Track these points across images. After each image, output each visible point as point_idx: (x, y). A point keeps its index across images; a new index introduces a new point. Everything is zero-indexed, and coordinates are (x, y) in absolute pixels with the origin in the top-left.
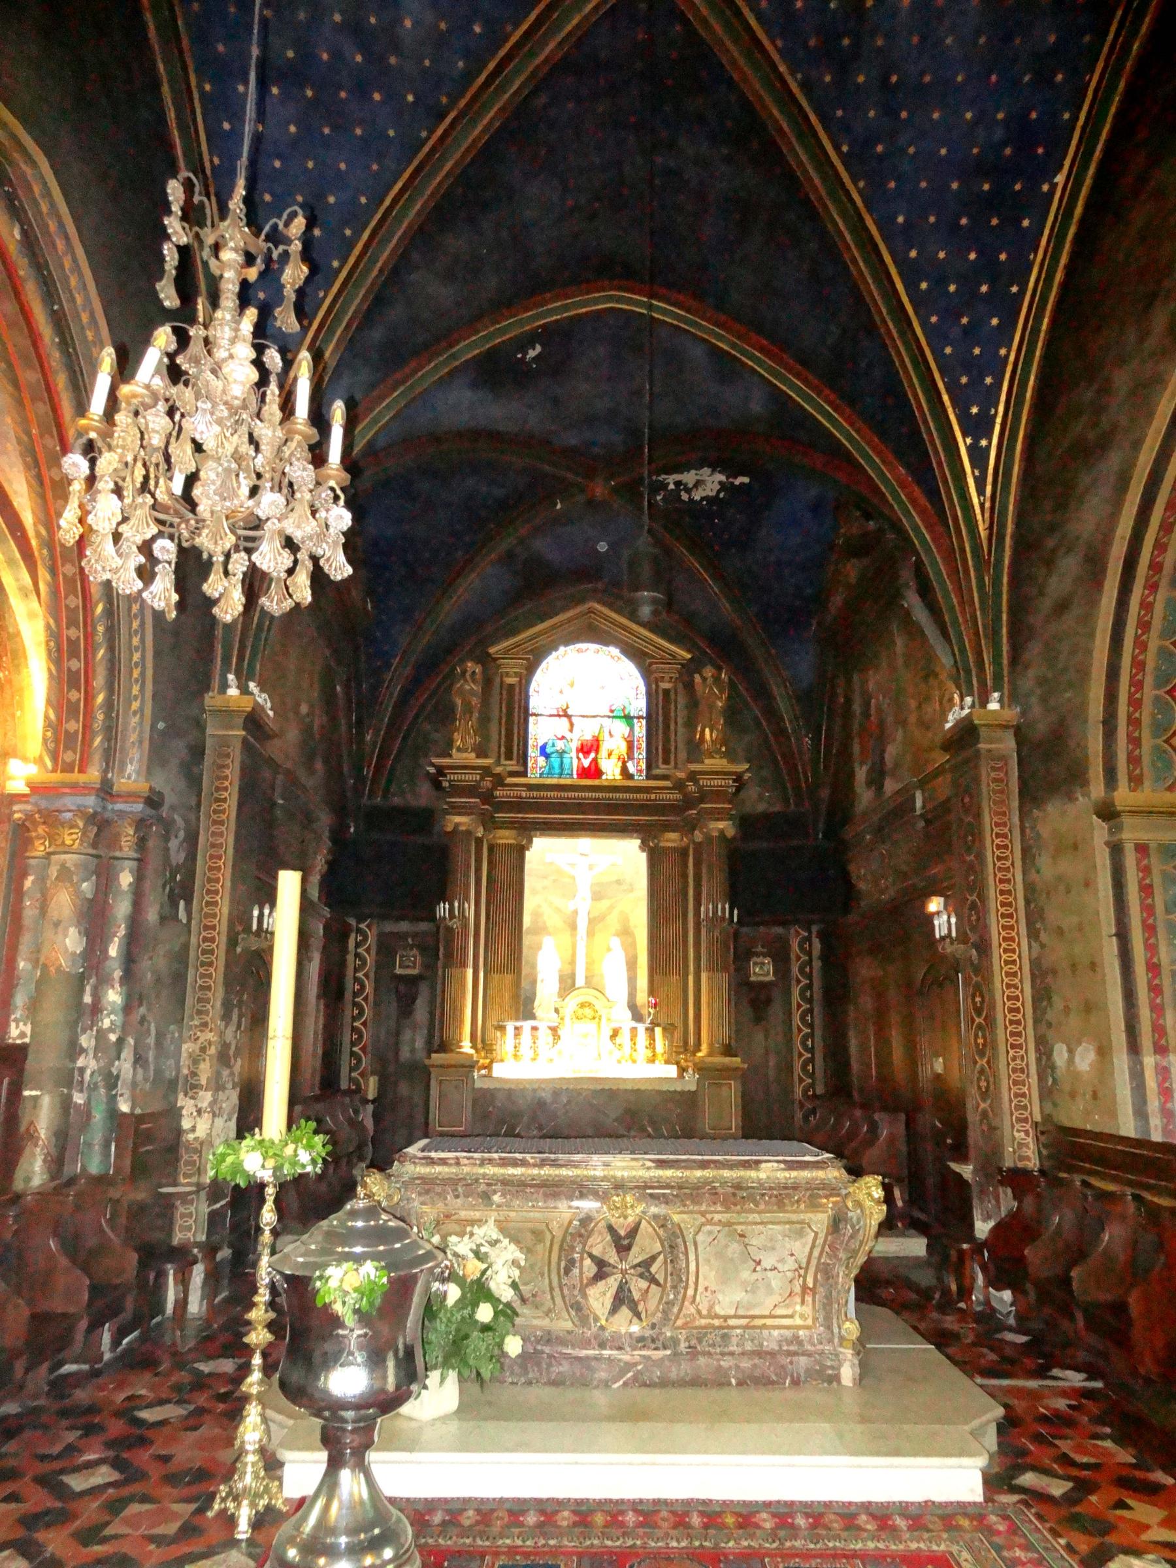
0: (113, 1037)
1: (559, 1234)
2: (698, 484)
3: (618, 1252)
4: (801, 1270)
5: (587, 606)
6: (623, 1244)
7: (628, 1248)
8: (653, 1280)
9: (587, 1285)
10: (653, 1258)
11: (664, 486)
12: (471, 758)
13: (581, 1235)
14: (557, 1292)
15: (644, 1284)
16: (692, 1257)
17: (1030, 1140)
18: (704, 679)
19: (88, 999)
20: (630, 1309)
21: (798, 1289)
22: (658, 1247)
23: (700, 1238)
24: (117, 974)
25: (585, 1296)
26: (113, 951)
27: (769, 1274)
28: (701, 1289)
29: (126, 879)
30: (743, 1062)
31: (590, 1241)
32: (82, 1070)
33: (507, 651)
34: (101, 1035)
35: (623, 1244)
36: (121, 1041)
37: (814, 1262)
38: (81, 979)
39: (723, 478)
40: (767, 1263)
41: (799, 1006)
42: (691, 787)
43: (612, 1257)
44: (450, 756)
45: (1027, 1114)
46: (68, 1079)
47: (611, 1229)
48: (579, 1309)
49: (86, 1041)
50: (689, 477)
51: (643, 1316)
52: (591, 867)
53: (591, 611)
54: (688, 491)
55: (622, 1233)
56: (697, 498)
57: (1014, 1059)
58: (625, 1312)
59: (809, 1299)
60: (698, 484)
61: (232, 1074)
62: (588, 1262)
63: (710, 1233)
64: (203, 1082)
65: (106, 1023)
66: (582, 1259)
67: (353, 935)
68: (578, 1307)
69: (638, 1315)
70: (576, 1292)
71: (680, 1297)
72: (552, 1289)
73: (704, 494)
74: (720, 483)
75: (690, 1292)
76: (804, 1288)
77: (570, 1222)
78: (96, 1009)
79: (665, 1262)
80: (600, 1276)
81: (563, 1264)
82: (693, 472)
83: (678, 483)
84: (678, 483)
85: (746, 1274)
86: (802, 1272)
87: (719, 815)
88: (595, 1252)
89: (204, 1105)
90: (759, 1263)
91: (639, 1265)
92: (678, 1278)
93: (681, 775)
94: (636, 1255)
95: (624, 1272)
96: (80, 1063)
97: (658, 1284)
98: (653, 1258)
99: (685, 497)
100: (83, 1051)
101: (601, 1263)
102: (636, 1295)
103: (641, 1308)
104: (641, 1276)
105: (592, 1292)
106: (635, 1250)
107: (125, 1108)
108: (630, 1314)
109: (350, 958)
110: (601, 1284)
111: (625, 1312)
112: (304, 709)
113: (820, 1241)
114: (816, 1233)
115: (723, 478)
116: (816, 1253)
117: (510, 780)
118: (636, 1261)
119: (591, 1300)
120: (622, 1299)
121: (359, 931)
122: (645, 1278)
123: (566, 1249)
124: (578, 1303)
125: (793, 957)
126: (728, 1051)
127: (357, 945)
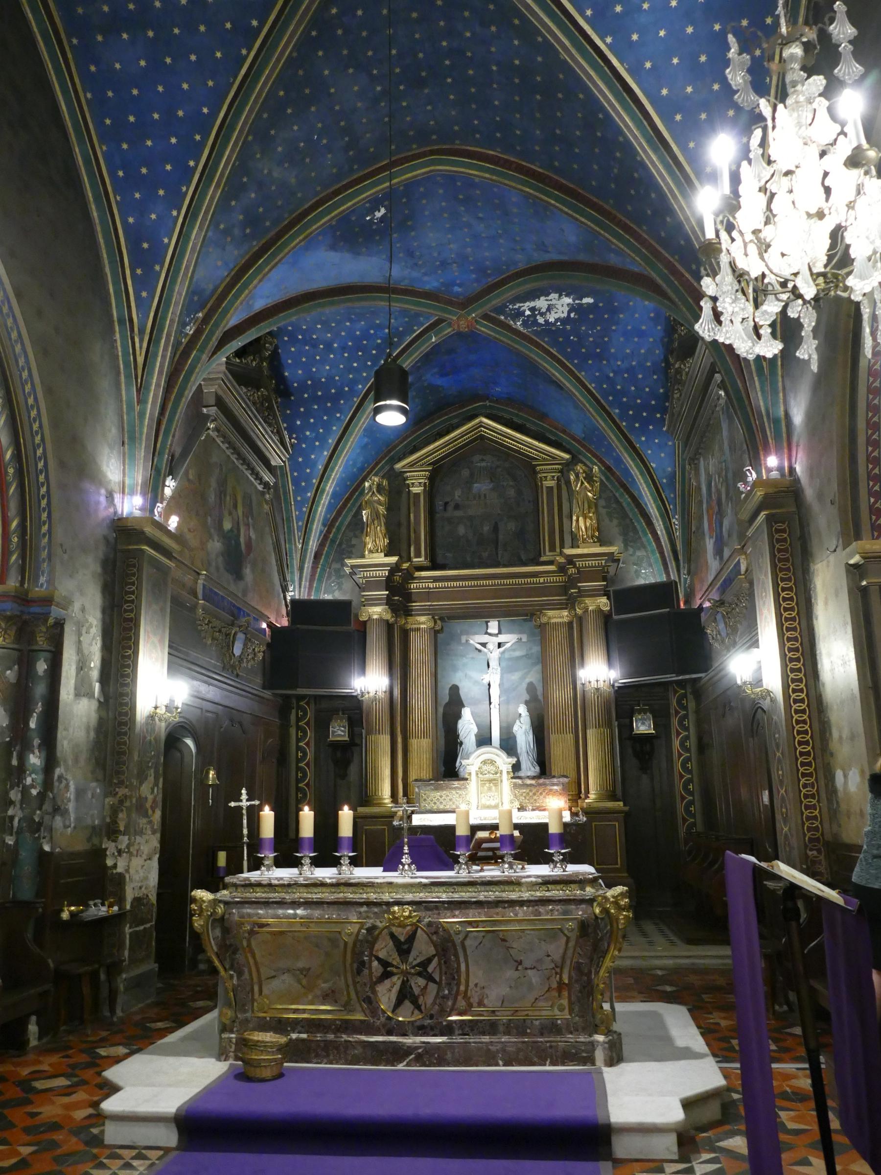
0: (34, 792)
1: (350, 941)
2: (549, 309)
3: (399, 955)
4: (559, 967)
5: (477, 421)
6: (404, 948)
7: (408, 952)
8: (430, 978)
9: (376, 983)
10: (429, 960)
11: (519, 314)
12: (380, 558)
13: (367, 942)
14: (351, 988)
15: (421, 982)
16: (462, 959)
17: (822, 857)
18: (577, 476)
19: (15, 762)
20: (412, 1002)
21: (555, 985)
22: (432, 951)
23: (468, 943)
24: (36, 742)
25: (374, 992)
26: (33, 725)
27: (529, 972)
28: (471, 985)
29: (42, 667)
30: (625, 805)
31: (377, 947)
32: (12, 818)
33: (412, 465)
34: (25, 791)
35: (404, 948)
36: (42, 796)
37: (568, 962)
38: (9, 746)
40: (527, 963)
41: (680, 755)
42: (572, 571)
43: (395, 959)
44: (363, 557)
45: (818, 835)
47: (392, 936)
48: (370, 1002)
50: (541, 303)
51: (423, 1008)
52: (500, 645)
53: (481, 424)
54: (542, 314)
55: (402, 939)
56: (552, 320)
57: (805, 786)
58: (407, 1004)
59: (565, 993)
60: (549, 309)
61: (150, 822)
62: (375, 963)
63: (476, 938)
64: (122, 828)
65: (29, 781)
66: (371, 962)
67: (294, 711)
68: (369, 1000)
69: (418, 1007)
70: (367, 989)
71: (454, 992)
72: (348, 986)
73: (557, 316)
74: (568, 305)
75: (462, 988)
76: (561, 984)
77: (359, 931)
79: (439, 964)
80: (387, 975)
81: (355, 965)
82: (542, 298)
83: (532, 309)
84: (532, 309)
85: (510, 973)
86: (558, 970)
87: (594, 593)
88: (381, 955)
89: (123, 846)
90: (520, 963)
91: (418, 965)
92: (452, 976)
93: (562, 560)
94: (415, 957)
95: (406, 973)
96: (10, 812)
97: (434, 981)
98: (429, 960)
99: (541, 320)
100: (12, 803)
101: (384, 964)
102: (416, 991)
103: (421, 1001)
104: (419, 974)
105: (381, 989)
106: (413, 953)
107: (47, 848)
108: (412, 1007)
109: (293, 731)
110: (387, 983)
111: (407, 1004)
112: (227, 525)
113: (572, 944)
114: (568, 939)
115: (568, 300)
116: (570, 953)
117: (417, 574)
118: (415, 963)
119: (379, 995)
120: (405, 995)
121: (299, 707)
122: (424, 977)
123: (357, 955)
124: (369, 998)
125: (672, 711)
127: (298, 720)
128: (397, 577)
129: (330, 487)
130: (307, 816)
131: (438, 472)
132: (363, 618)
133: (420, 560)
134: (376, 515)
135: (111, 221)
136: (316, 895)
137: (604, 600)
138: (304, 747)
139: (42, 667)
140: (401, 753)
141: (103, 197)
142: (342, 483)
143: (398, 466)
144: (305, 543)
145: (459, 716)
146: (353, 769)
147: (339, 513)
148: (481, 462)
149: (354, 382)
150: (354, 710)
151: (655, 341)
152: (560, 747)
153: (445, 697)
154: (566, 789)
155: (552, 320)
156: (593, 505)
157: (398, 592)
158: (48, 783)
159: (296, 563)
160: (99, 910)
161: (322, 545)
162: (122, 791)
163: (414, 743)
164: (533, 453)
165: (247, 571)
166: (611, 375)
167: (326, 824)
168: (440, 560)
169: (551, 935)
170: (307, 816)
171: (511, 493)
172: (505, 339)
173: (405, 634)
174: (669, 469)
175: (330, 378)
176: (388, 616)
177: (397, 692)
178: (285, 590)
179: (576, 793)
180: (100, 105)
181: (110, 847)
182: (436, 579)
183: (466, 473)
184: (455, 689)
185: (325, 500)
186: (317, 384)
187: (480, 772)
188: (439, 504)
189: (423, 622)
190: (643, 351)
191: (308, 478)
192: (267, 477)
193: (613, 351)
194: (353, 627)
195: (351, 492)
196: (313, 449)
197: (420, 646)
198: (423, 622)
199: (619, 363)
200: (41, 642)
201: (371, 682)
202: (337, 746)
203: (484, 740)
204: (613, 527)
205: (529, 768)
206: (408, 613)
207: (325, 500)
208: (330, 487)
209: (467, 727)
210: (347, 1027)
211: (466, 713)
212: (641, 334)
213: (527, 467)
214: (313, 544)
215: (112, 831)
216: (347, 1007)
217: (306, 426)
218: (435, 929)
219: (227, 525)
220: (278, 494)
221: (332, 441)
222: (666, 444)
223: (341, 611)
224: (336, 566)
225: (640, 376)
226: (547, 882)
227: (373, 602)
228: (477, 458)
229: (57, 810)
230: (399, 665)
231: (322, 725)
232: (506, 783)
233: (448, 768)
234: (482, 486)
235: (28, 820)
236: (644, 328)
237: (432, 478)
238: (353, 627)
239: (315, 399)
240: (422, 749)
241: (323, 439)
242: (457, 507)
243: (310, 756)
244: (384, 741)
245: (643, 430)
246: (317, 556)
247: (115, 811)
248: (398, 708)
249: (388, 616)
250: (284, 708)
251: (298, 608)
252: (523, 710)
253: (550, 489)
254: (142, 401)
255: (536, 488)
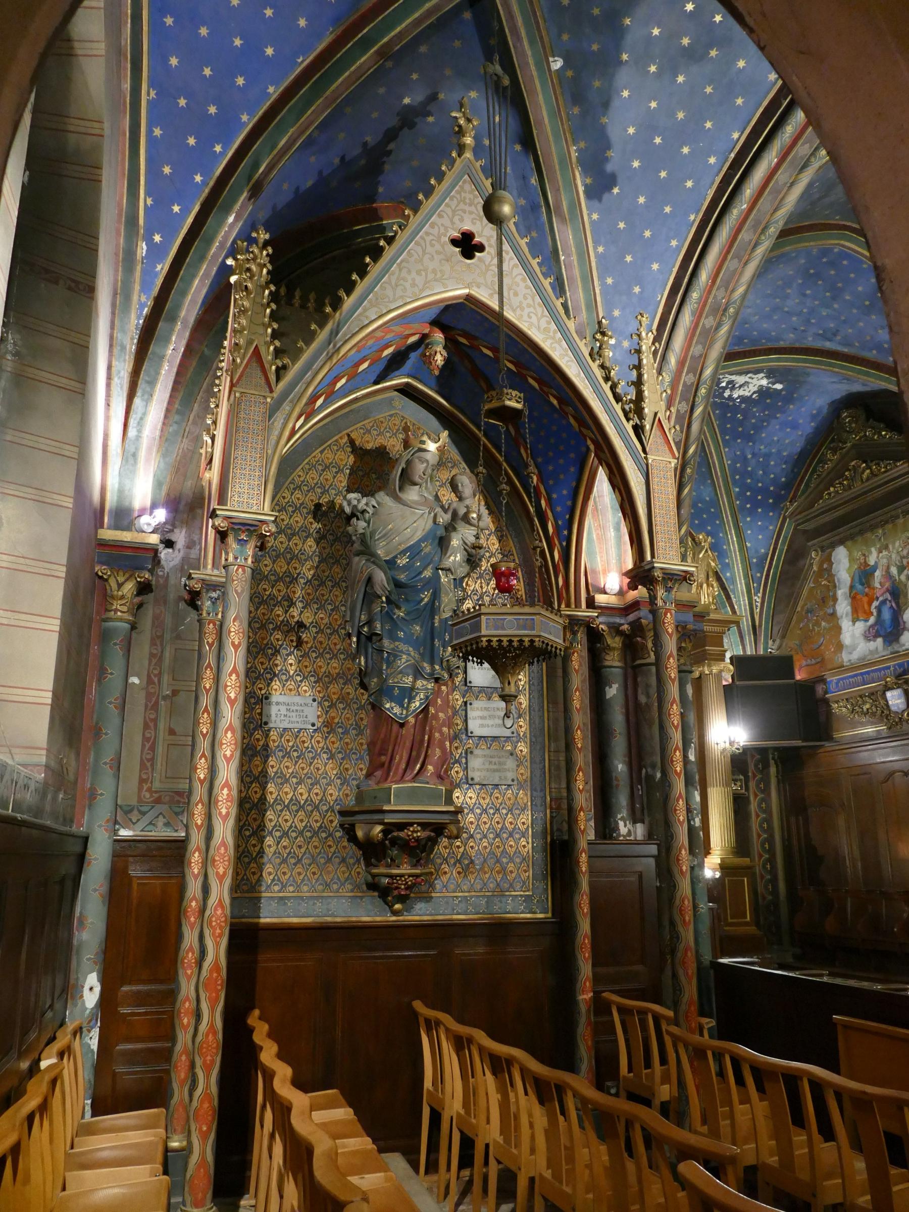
39: (764, 382)
56: (735, 396)
115: (764, 382)
151: (801, 436)
155: (735, 396)
166: (749, 456)
174: (763, 551)
190: (787, 441)
193: (763, 435)
199: (762, 447)
212: (795, 426)
222: (767, 528)
225: (772, 463)
236: (801, 421)
245: (752, 512)
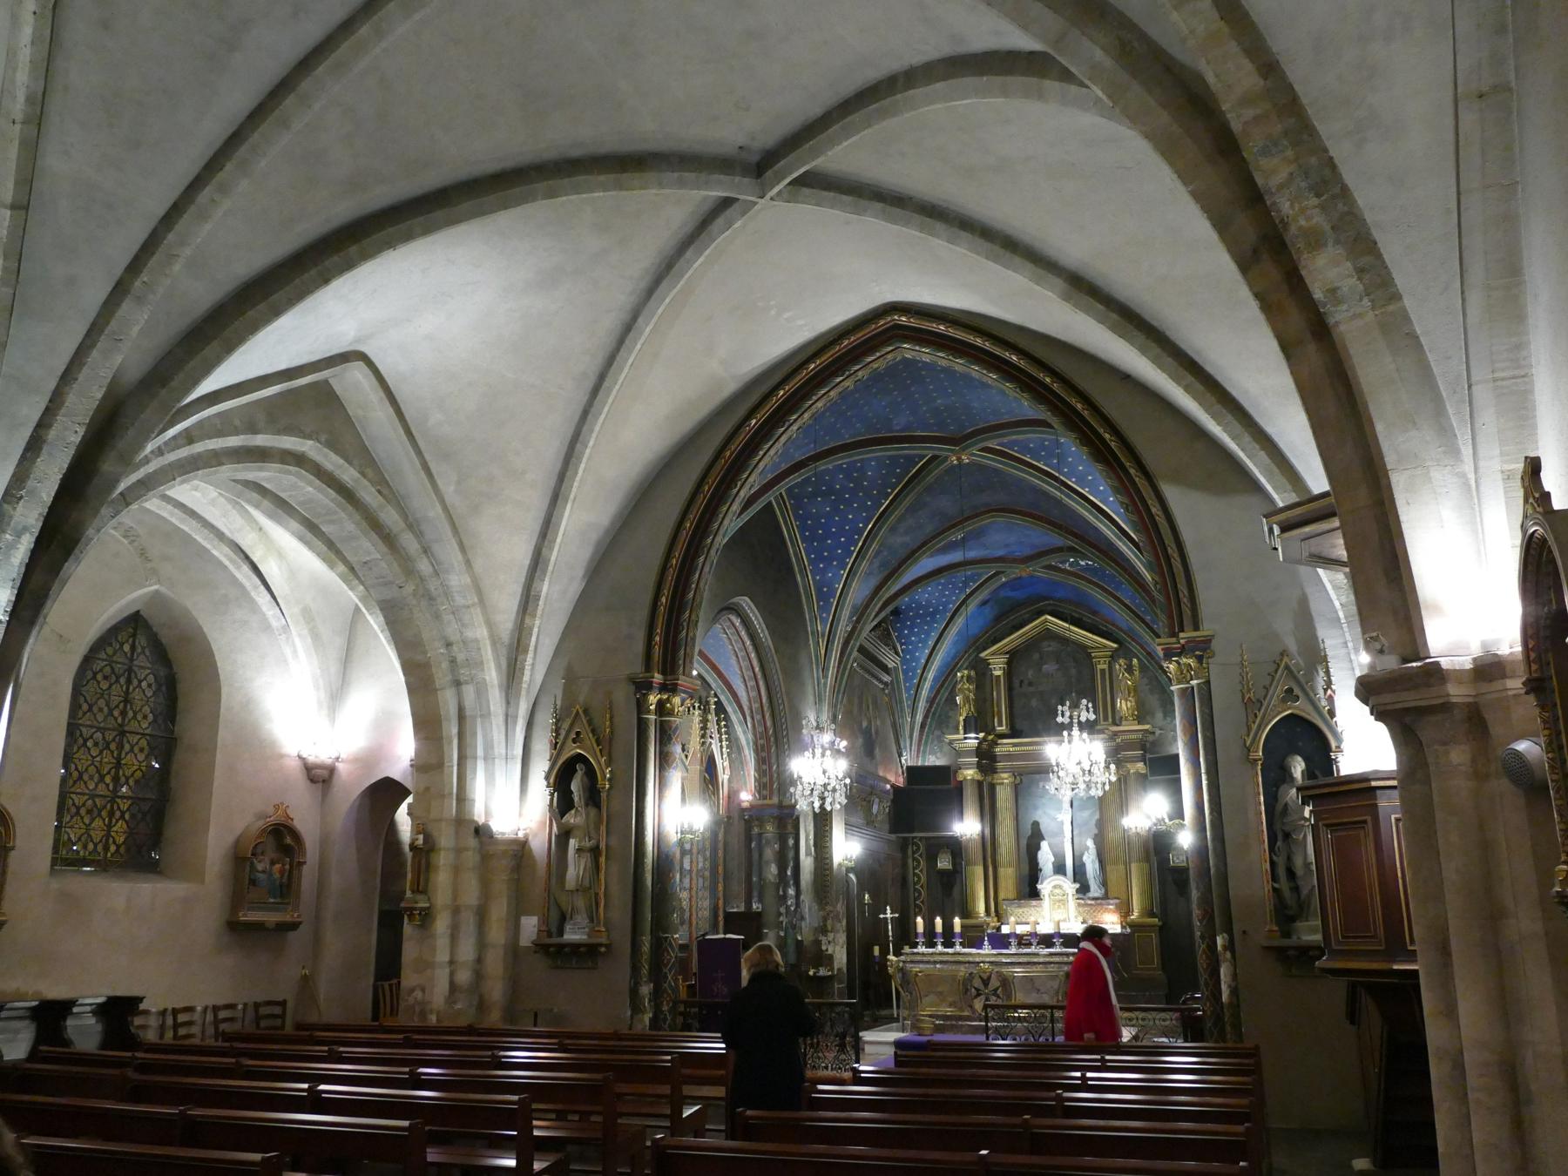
6: (986, 982)
29: (791, 842)
33: (993, 654)
34: (788, 908)
43: (982, 987)
46: (779, 925)
49: (782, 910)
78: (785, 897)
80: (979, 995)
109: (910, 861)
112: (865, 724)
126: (1152, 914)
128: (985, 746)
129: (930, 675)
130: (938, 921)
131: (1014, 657)
132: (960, 778)
133: (1002, 729)
134: (966, 699)
135: (806, 580)
136: (945, 958)
137: (1141, 765)
138: (919, 873)
139: (791, 842)
140: (992, 881)
141: (803, 570)
142: (940, 671)
143: (983, 655)
144: (913, 716)
145: (1039, 848)
146: (956, 890)
147: (938, 692)
148: (1049, 647)
149: (948, 603)
150: (956, 847)
152: (1115, 873)
153: (1027, 830)
154: (1119, 909)
156: (1135, 690)
157: (987, 759)
158: (798, 904)
159: (907, 733)
160: (823, 972)
161: (926, 717)
162: (829, 908)
163: (1002, 871)
164: (1089, 643)
165: (877, 751)
167: (948, 926)
168: (1018, 726)
169: (1053, 978)
170: (938, 921)
171: (1073, 671)
172: (1057, 577)
173: (992, 787)
175: (927, 601)
176: (979, 777)
177: (987, 831)
178: (900, 755)
179: (1125, 910)
180: (802, 528)
181: (823, 939)
182: (1015, 745)
183: (1036, 656)
184: (1036, 825)
185: (927, 685)
186: (920, 606)
187: (1052, 894)
188: (1016, 683)
189: (1006, 778)
191: (915, 669)
192: (886, 678)
194: (953, 785)
195: (946, 679)
196: (917, 649)
197: (1004, 795)
198: (1006, 778)
200: (790, 828)
201: (967, 827)
202: (943, 873)
203: (1060, 869)
204: (1153, 701)
205: (1095, 890)
206: (994, 771)
207: (927, 685)
208: (930, 675)
209: (1046, 857)
210: (961, 1018)
211: (1044, 845)
213: (1084, 650)
214: (919, 718)
215: (824, 930)
216: (961, 1010)
217: (912, 633)
218: (999, 974)
219: (865, 724)
220: (893, 687)
221: (931, 643)
223: (943, 775)
224: (937, 733)
226: (1051, 954)
227: (968, 765)
228: (1045, 643)
229: (802, 918)
230: (988, 812)
231: (932, 859)
232: (1072, 903)
233: (1030, 891)
234: (1050, 667)
235: (790, 922)
237: (1009, 663)
238: (953, 785)
239: (918, 616)
240: (1008, 876)
241: (924, 642)
242: (1030, 684)
243: (923, 879)
244: (979, 870)
246: (923, 726)
247: (825, 919)
248: (989, 845)
249: (979, 777)
250: (903, 846)
251: (913, 773)
252: (1090, 843)
253: (1103, 671)
254: (825, 677)
255: (1092, 667)
